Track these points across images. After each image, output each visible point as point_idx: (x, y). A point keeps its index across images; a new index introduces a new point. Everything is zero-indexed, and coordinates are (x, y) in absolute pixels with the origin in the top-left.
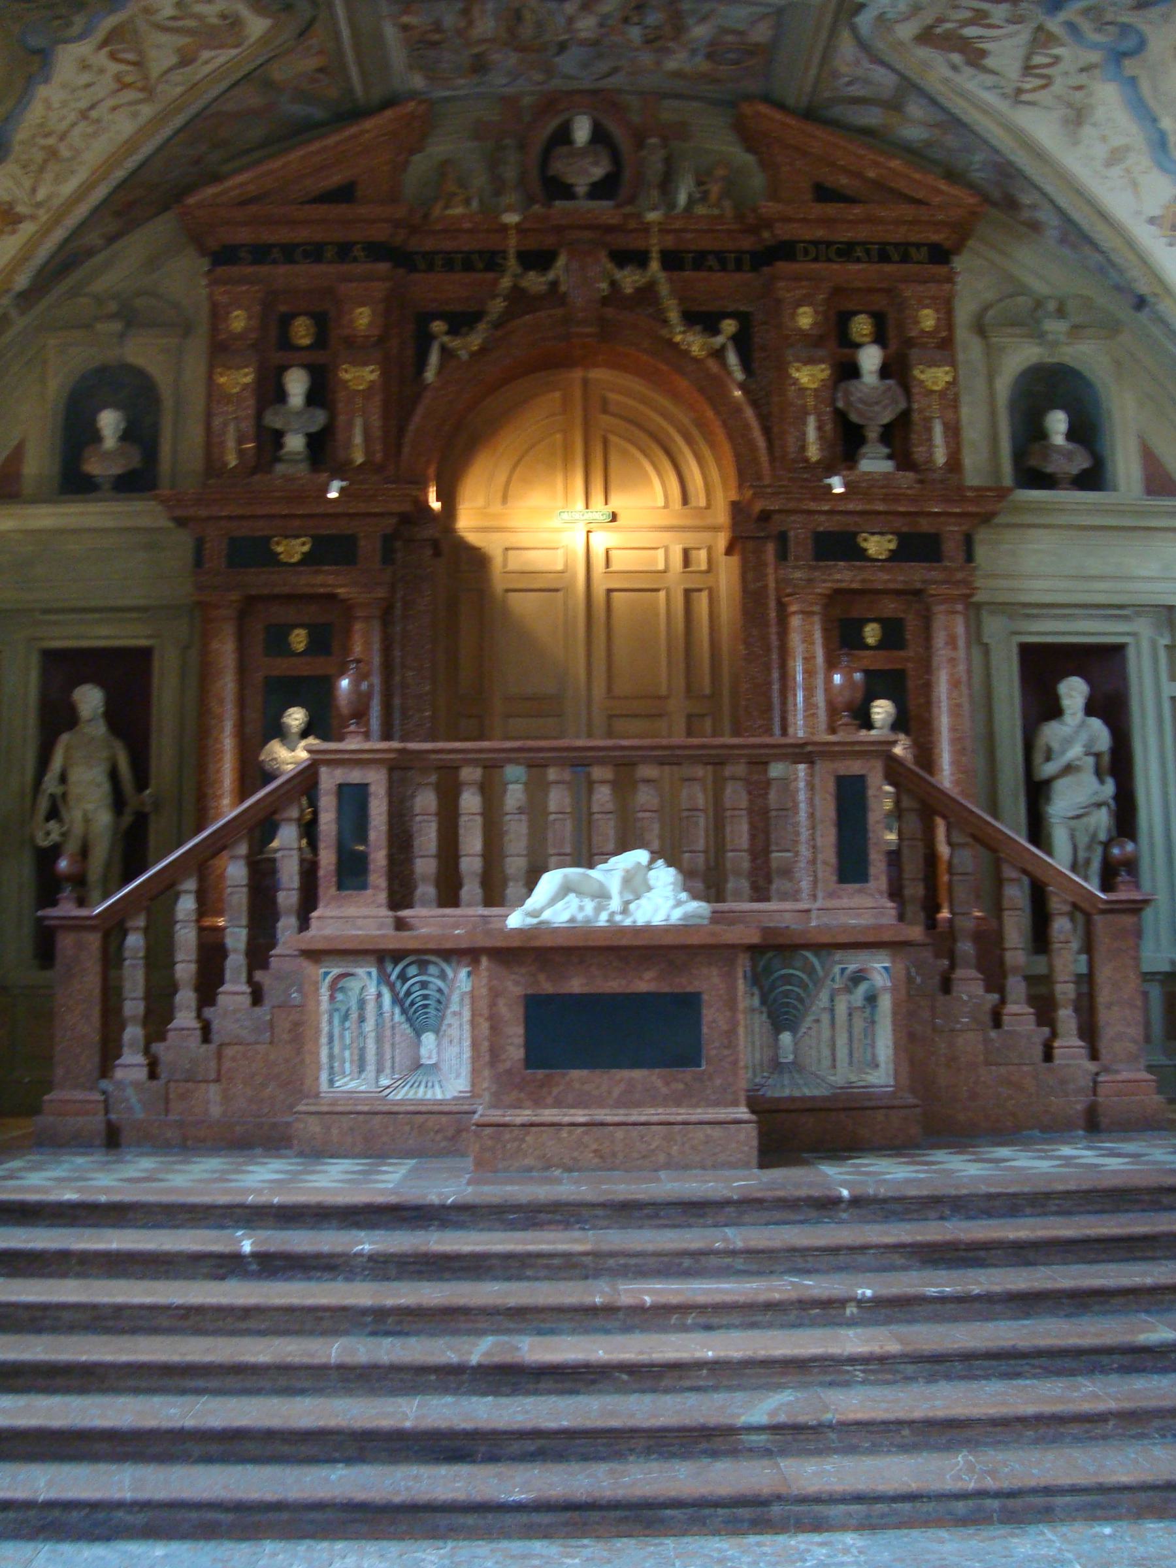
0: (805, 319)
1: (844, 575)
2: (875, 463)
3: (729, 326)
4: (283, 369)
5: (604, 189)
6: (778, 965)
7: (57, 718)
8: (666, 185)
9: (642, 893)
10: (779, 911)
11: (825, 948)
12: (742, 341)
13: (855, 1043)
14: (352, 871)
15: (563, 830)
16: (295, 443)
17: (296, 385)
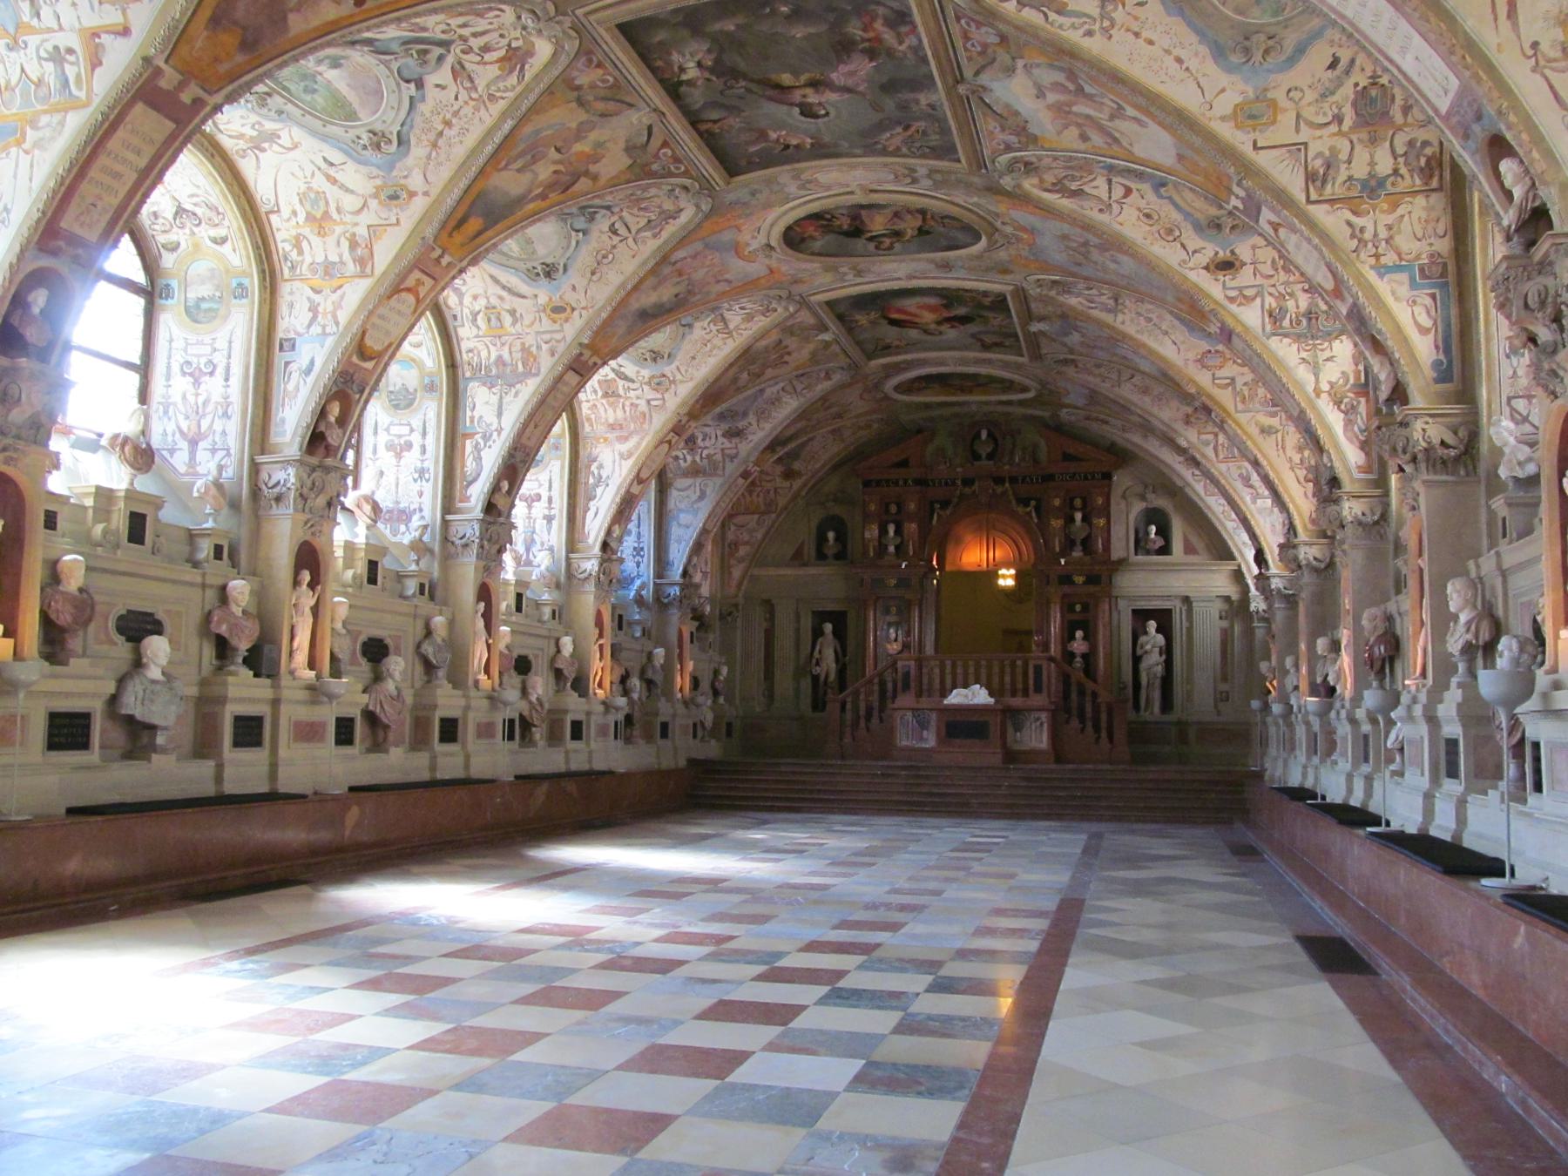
0: (1057, 502)
1: (1066, 589)
2: (1077, 553)
3: (1033, 503)
4: (887, 522)
5: (990, 457)
6: (1012, 717)
7: (817, 633)
8: (1012, 453)
9: (978, 695)
10: (1017, 702)
11: (1030, 710)
12: (1037, 509)
13: (1036, 737)
14: (906, 687)
15: (960, 678)
16: (892, 549)
17: (891, 529)
